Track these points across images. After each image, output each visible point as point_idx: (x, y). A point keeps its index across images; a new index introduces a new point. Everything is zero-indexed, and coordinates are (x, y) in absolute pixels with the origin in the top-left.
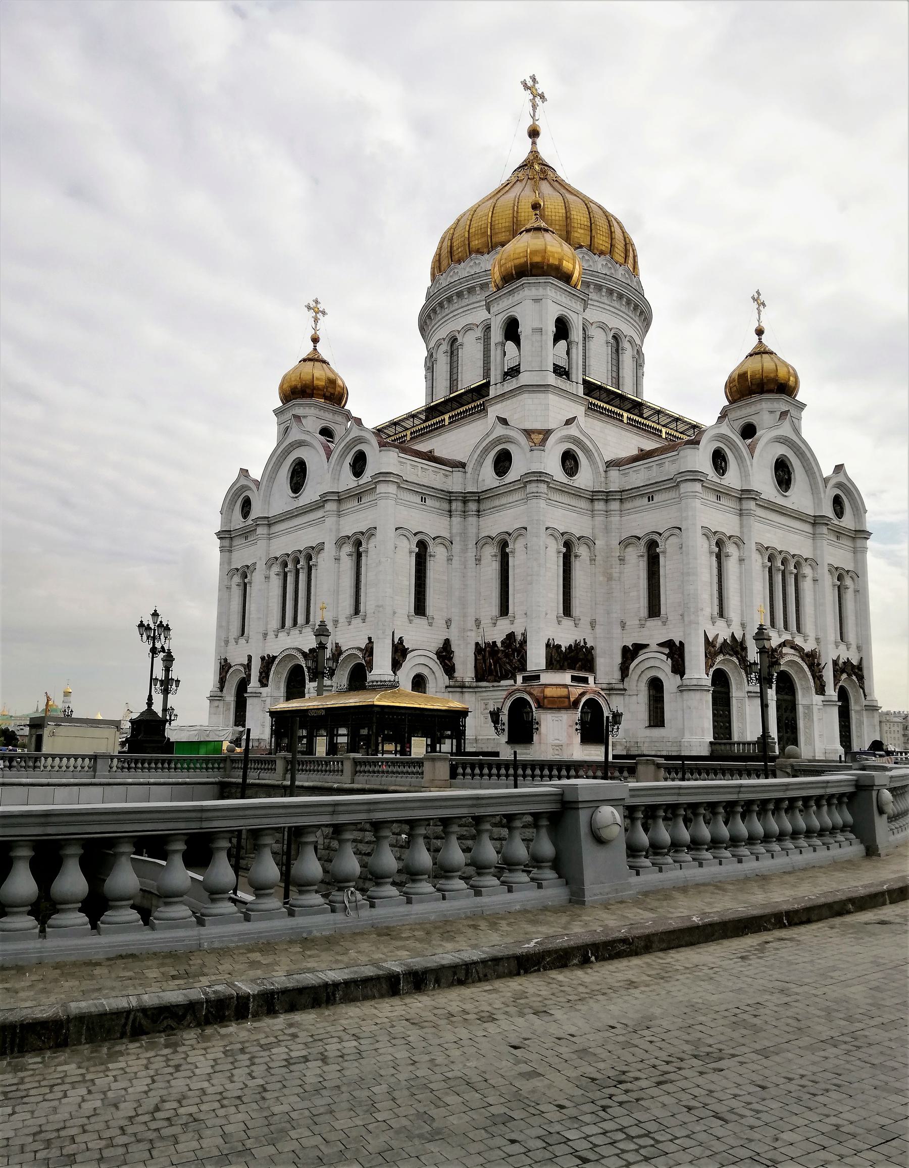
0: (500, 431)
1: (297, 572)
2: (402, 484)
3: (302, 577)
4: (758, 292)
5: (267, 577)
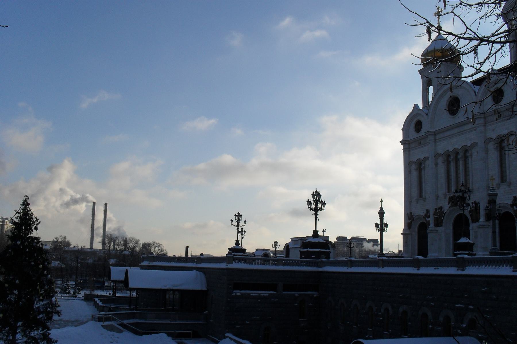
1: (457, 160)
5: (436, 165)
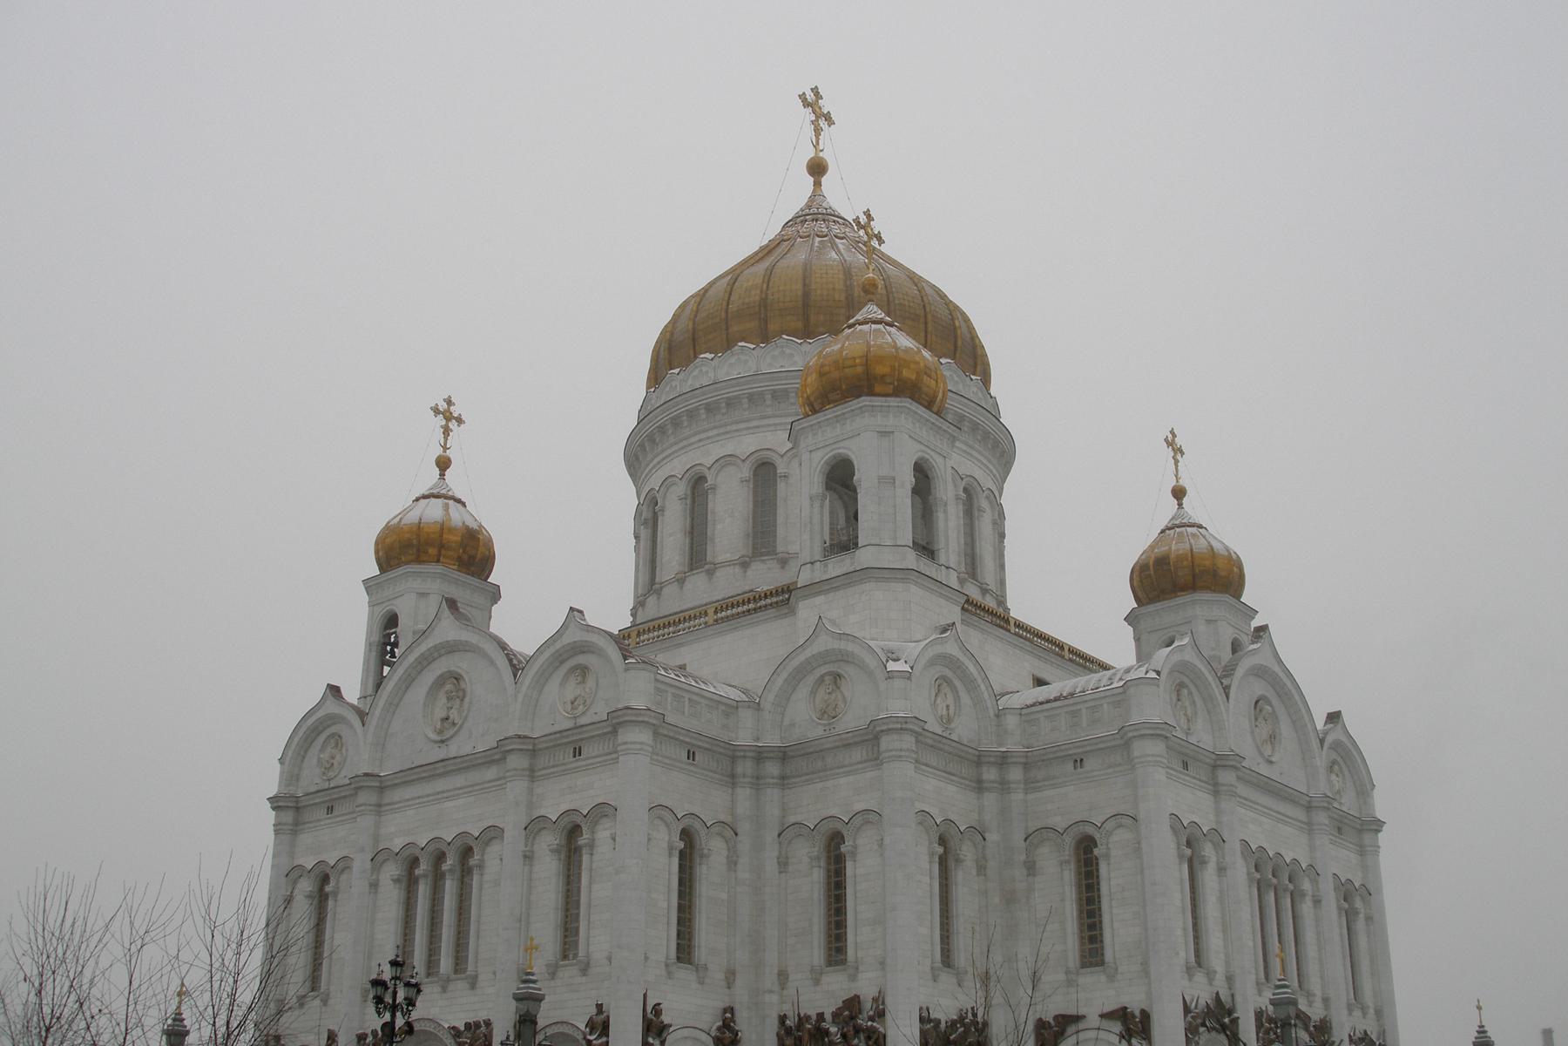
1: (438, 878)
3: (450, 886)
4: (1172, 432)
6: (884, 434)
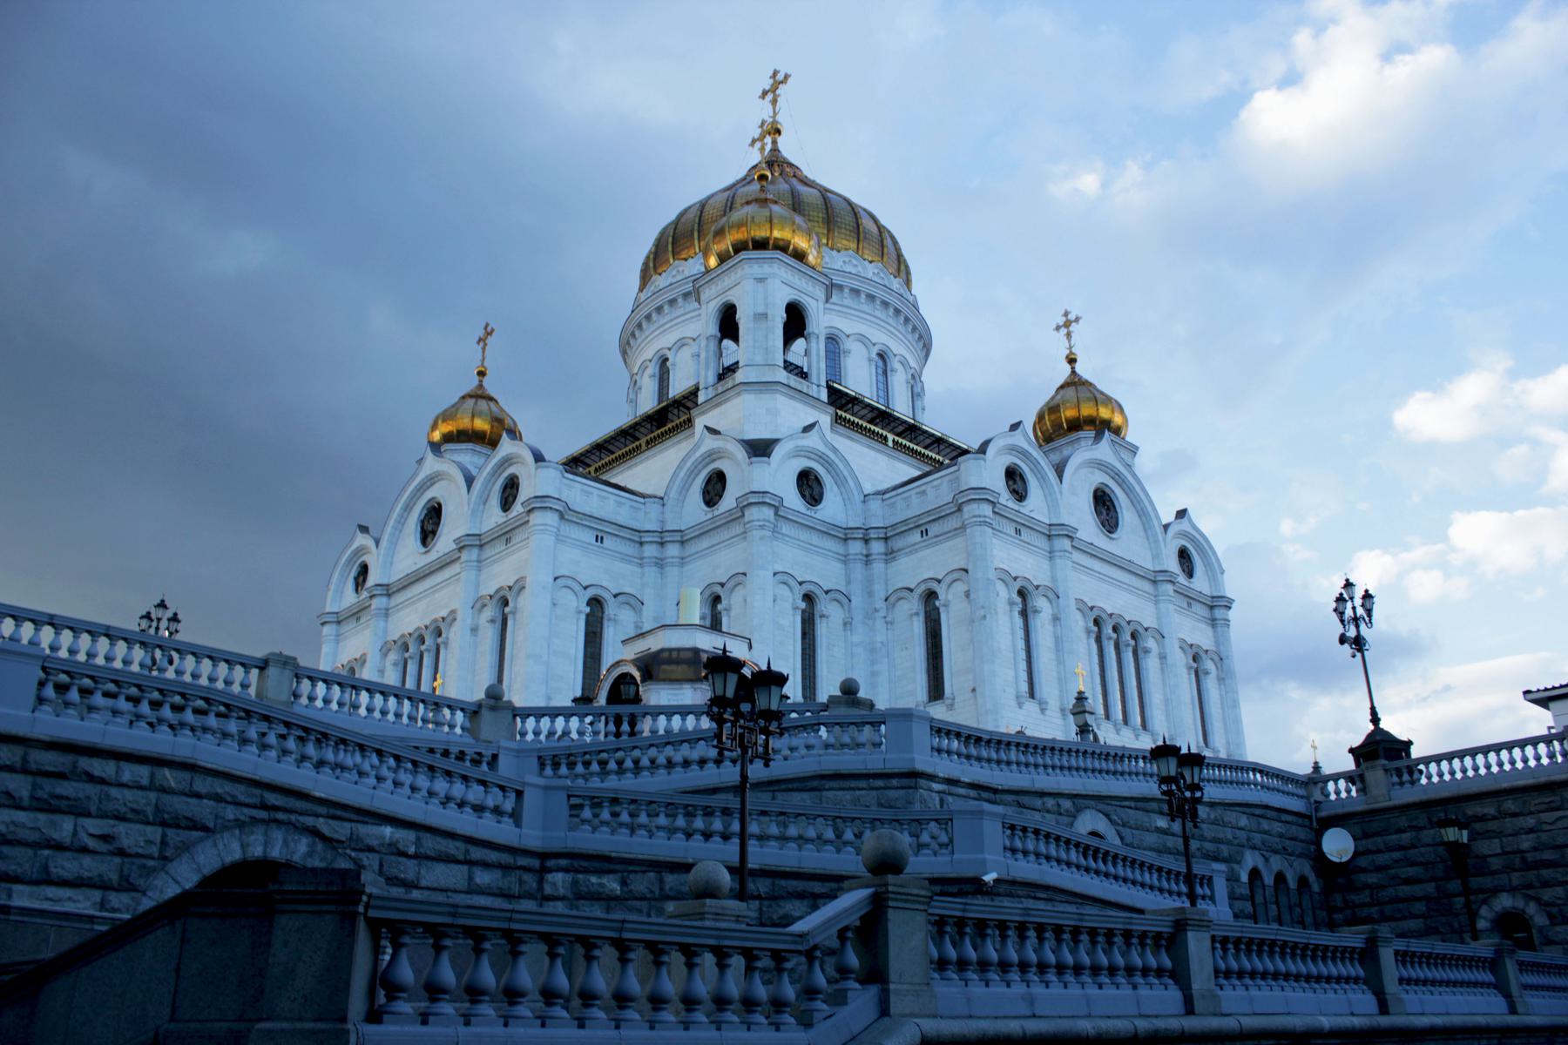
0: (711, 443)
2: (566, 514)
6: (761, 280)
